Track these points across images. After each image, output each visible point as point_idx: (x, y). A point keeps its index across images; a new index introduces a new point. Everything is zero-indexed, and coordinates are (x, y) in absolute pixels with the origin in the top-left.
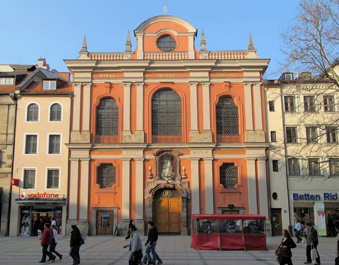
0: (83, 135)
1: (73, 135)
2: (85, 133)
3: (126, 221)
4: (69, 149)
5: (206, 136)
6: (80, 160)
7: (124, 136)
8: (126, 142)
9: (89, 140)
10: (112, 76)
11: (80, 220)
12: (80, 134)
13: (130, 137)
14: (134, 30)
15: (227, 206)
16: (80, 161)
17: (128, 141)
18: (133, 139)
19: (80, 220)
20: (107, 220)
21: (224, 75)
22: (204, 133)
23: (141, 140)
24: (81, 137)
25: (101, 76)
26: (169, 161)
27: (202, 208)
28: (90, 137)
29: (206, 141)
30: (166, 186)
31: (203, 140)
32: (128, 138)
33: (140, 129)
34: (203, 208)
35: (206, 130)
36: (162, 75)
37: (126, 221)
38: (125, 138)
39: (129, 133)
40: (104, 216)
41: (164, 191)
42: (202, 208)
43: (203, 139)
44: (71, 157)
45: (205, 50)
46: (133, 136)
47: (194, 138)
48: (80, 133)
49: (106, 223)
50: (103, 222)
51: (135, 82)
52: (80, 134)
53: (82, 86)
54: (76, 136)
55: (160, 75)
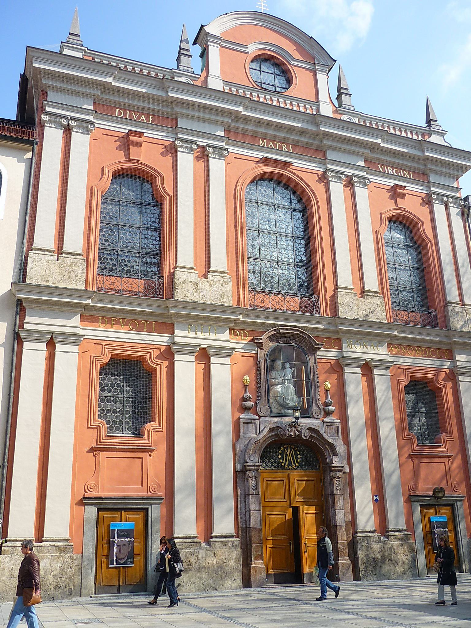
0: (65, 264)
1: (37, 260)
2: (71, 260)
3: (190, 540)
4: (20, 302)
5: (373, 306)
6: (52, 338)
7: (181, 280)
8: (187, 299)
9: (84, 279)
10: (148, 119)
11: (47, 541)
12: (58, 260)
13: (196, 286)
14: (202, 26)
15: (431, 493)
16: (51, 344)
17: (192, 297)
18: (204, 292)
19: (47, 541)
20: (129, 539)
21: (392, 171)
22: (369, 298)
23: (226, 297)
24: (61, 269)
25: (120, 113)
26: (288, 365)
27: (378, 498)
28: (85, 271)
29: (373, 318)
30: (292, 434)
31: (367, 315)
32: (191, 287)
33: (221, 270)
34: (378, 498)
35: (369, 292)
36: (265, 141)
37: (190, 540)
38: (184, 285)
39: (194, 277)
40: (119, 528)
41: (280, 449)
42: (375, 498)
43: (367, 312)
44: (26, 326)
45: (352, 108)
46: (205, 285)
47: (349, 307)
48: (56, 257)
49: (125, 551)
50: (116, 547)
51: (205, 144)
52: (58, 260)
53: (68, 130)
54: (45, 263)
55: (264, 143)
